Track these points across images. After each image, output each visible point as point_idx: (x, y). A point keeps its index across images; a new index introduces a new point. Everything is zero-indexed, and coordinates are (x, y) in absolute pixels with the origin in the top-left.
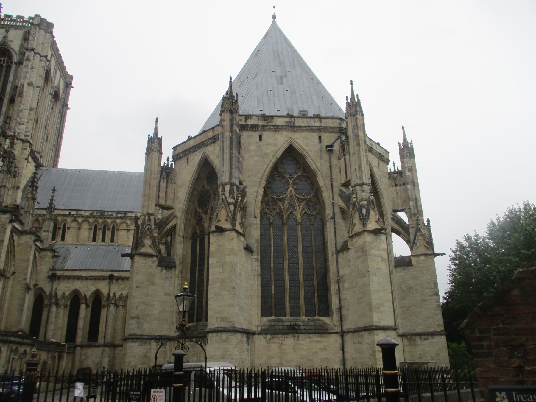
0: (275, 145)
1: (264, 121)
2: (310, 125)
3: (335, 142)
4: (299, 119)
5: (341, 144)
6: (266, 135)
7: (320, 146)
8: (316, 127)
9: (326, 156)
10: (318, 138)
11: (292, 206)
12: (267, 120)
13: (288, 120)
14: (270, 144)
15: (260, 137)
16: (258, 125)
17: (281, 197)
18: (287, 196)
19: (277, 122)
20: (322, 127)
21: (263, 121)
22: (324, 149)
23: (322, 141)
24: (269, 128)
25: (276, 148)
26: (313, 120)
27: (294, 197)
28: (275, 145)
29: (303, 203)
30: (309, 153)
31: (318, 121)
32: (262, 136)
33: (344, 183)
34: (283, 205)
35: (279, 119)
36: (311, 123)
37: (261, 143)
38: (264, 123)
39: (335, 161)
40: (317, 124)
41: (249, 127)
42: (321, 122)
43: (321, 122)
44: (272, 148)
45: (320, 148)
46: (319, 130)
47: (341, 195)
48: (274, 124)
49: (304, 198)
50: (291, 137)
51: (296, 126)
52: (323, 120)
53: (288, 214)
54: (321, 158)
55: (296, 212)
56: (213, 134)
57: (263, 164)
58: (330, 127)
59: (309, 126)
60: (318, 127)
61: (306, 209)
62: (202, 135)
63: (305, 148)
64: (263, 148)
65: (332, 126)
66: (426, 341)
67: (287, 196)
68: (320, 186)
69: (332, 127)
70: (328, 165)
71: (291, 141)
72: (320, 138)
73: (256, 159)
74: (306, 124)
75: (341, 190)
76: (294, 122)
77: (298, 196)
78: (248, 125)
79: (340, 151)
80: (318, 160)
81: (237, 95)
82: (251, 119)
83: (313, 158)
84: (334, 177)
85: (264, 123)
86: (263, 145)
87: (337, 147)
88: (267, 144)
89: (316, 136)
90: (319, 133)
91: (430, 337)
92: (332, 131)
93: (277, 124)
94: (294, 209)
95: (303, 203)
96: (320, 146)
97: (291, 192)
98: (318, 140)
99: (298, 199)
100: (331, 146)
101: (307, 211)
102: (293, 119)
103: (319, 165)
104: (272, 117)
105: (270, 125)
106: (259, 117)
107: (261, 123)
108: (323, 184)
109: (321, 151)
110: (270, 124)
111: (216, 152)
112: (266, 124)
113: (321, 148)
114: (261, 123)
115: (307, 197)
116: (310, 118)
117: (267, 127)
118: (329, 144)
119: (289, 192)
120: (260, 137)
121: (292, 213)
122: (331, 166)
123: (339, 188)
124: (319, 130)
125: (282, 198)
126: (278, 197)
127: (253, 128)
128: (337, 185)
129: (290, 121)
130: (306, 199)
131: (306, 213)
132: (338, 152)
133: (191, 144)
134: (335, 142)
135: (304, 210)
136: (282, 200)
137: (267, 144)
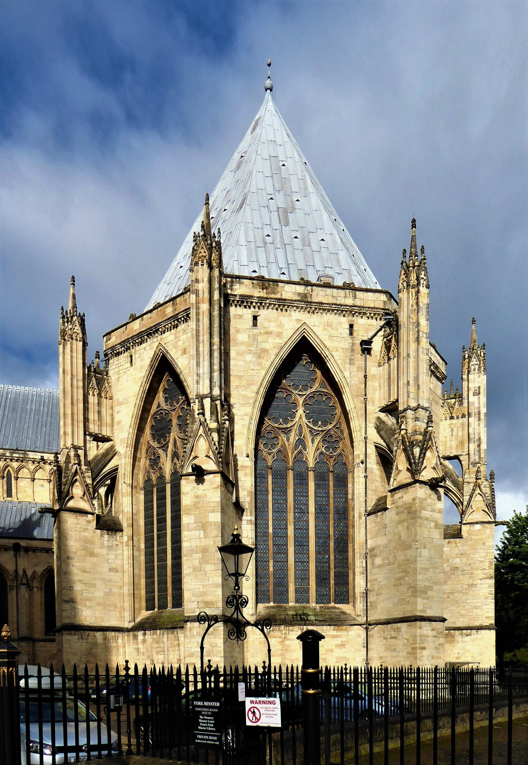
0: (279, 335)
1: (263, 289)
2: (338, 302)
3: (375, 335)
4: (319, 288)
5: (385, 339)
6: (264, 314)
7: (351, 341)
8: (346, 306)
9: (359, 357)
10: (348, 327)
11: (301, 442)
12: (267, 288)
13: (301, 289)
14: (271, 333)
15: (255, 318)
16: (251, 297)
17: (285, 426)
18: (294, 425)
19: (283, 293)
20: (357, 307)
21: (261, 290)
22: (358, 348)
23: (355, 333)
24: (270, 304)
25: (281, 341)
26: (342, 292)
27: (305, 428)
28: (279, 335)
29: (319, 438)
30: (333, 353)
31: (351, 296)
32: (258, 318)
33: (385, 407)
34: (288, 440)
35: (288, 287)
36: (338, 298)
37: (255, 331)
38: (263, 294)
39: (373, 370)
40: (349, 301)
41: (237, 299)
42: (355, 297)
43: (355, 297)
44: (274, 341)
45: (351, 344)
46: (351, 312)
47: (380, 427)
48: (278, 296)
49: (320, 429)
50: (305, 323)
51: (314, 303)
52: (358, 293)
53: (295, 454)
54: (351, 362)
55: (307, 450)
56: (175, 310)
57: (259, 368)
58: (369, 308)
59: (335, 304)
60: (351, 306)
61: (323, 447)
62: (154, 311)
63: (327, 343)
64: (260, 338)
65: (372, 306)
66: (468, 637)
67: (294, 425)
68: (348, 409)
69: (372, 308)
70: (362, 375)
71: (305, 329)
72: (351, 326)
73: (249, 358)
74: (331, 300)
75: (379, 418)
76: (311, 295)
77: (311, 426)
78: (236, 295)
79: (381, 351)
80: (347, 366)
81: (219, 232)
82: (240, 283)
83: (339, 362)
84: (368, 396)
85: (263, 294)
86: (260, 333)
87: (377, 345)
88: (266, 333)
89: (344, 321)
90: (350, 318)
91: (474, 632)
92: (372, 315)
93: (283, 297)
94: (305, 448)
95: (319, 438)
96: (351, 341)
97: (300, 418)
98: (348, 331)
99: (311, 431)
100: (369, 342)
101: (324, 450)
102: (309, 288)
103: (347, 374)
104: (276, 282)
105: (272, 298)
106: (255, 282)
107: (258, 293)
108: (353, 407)
109: (353, 350)
110: (273, 296)
111: (180, 343)
112: (265, 296)
113: (353, 344)
114: (258, 293)
115: (324, 428)
116: (338, 288)
117: (268, 301)
118: (365, 338)
119: (297, 419)
120: (255, 318)
121: (300, 452)
122: (365, 377)
123: (377, 415)
124: (351, 312)
125: (287, 428)
126: (281, 426)
127: (243, 302)
128: (374, 410)
129: (306, 292)
130: (322, 431)
131: (321, 453)
132: (378, 354)
133: (135, 329)
134: (375, 335)
135: (318, 449)
136: (287, 431)
137: (266, 333)
